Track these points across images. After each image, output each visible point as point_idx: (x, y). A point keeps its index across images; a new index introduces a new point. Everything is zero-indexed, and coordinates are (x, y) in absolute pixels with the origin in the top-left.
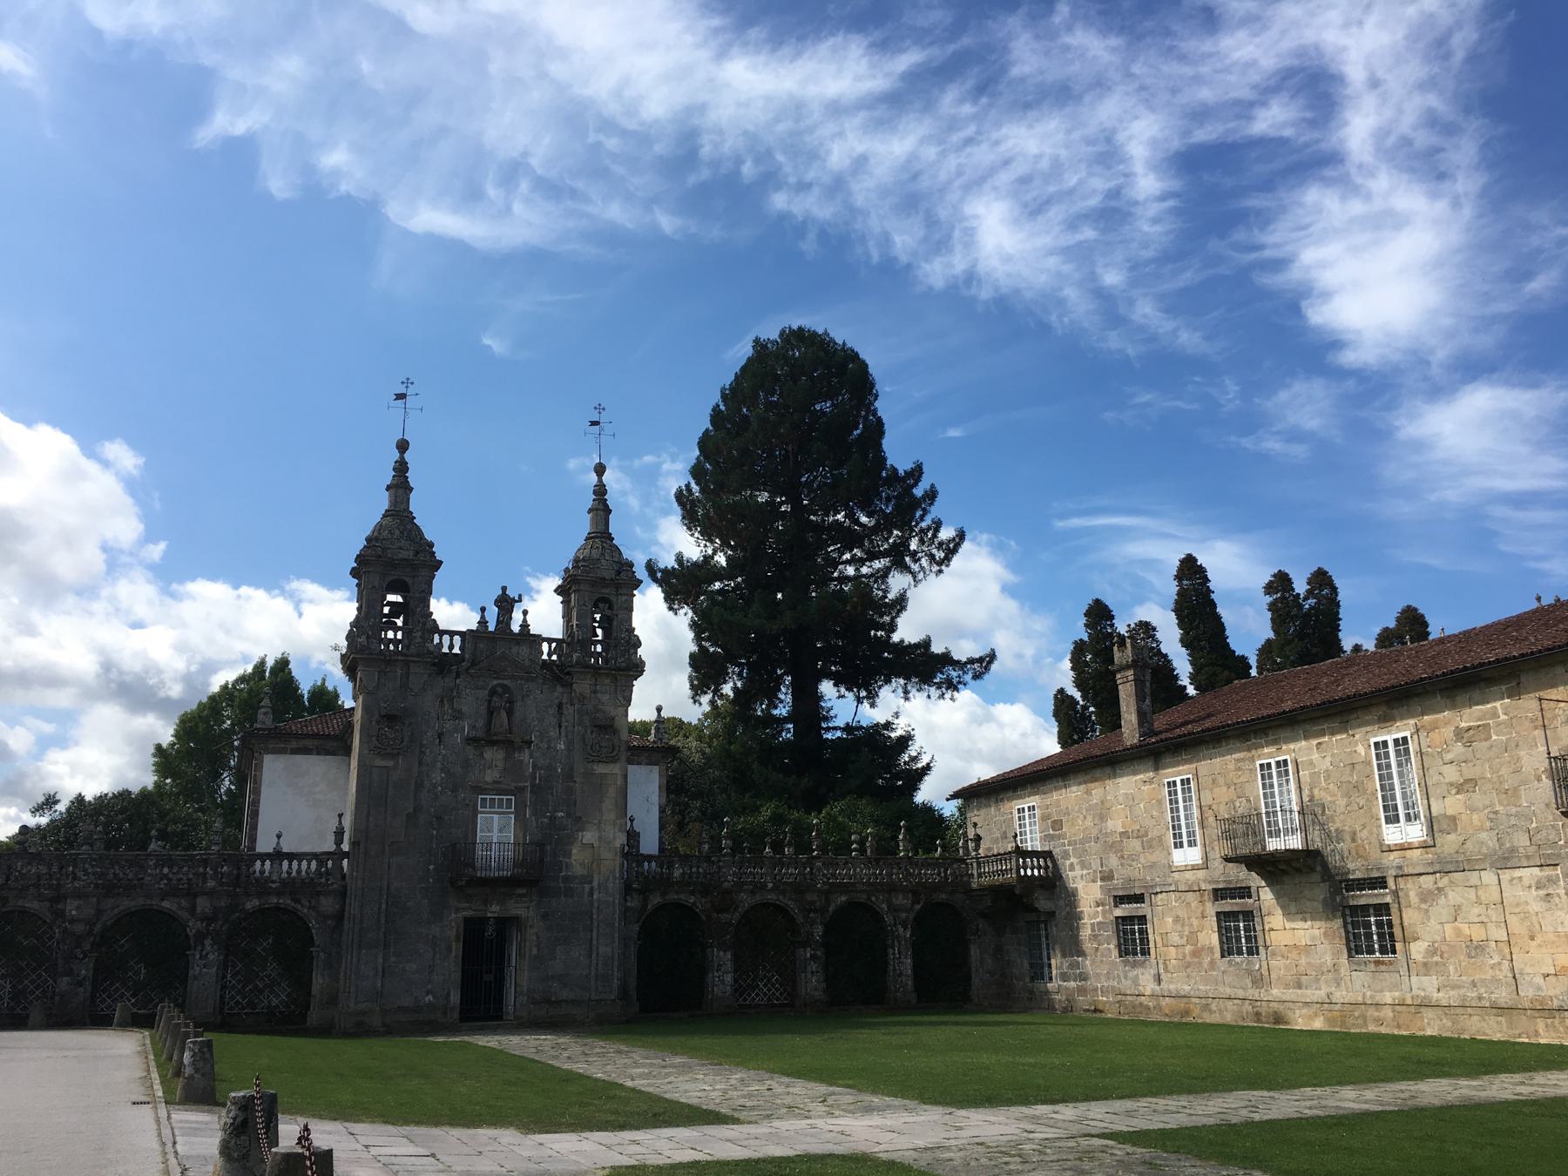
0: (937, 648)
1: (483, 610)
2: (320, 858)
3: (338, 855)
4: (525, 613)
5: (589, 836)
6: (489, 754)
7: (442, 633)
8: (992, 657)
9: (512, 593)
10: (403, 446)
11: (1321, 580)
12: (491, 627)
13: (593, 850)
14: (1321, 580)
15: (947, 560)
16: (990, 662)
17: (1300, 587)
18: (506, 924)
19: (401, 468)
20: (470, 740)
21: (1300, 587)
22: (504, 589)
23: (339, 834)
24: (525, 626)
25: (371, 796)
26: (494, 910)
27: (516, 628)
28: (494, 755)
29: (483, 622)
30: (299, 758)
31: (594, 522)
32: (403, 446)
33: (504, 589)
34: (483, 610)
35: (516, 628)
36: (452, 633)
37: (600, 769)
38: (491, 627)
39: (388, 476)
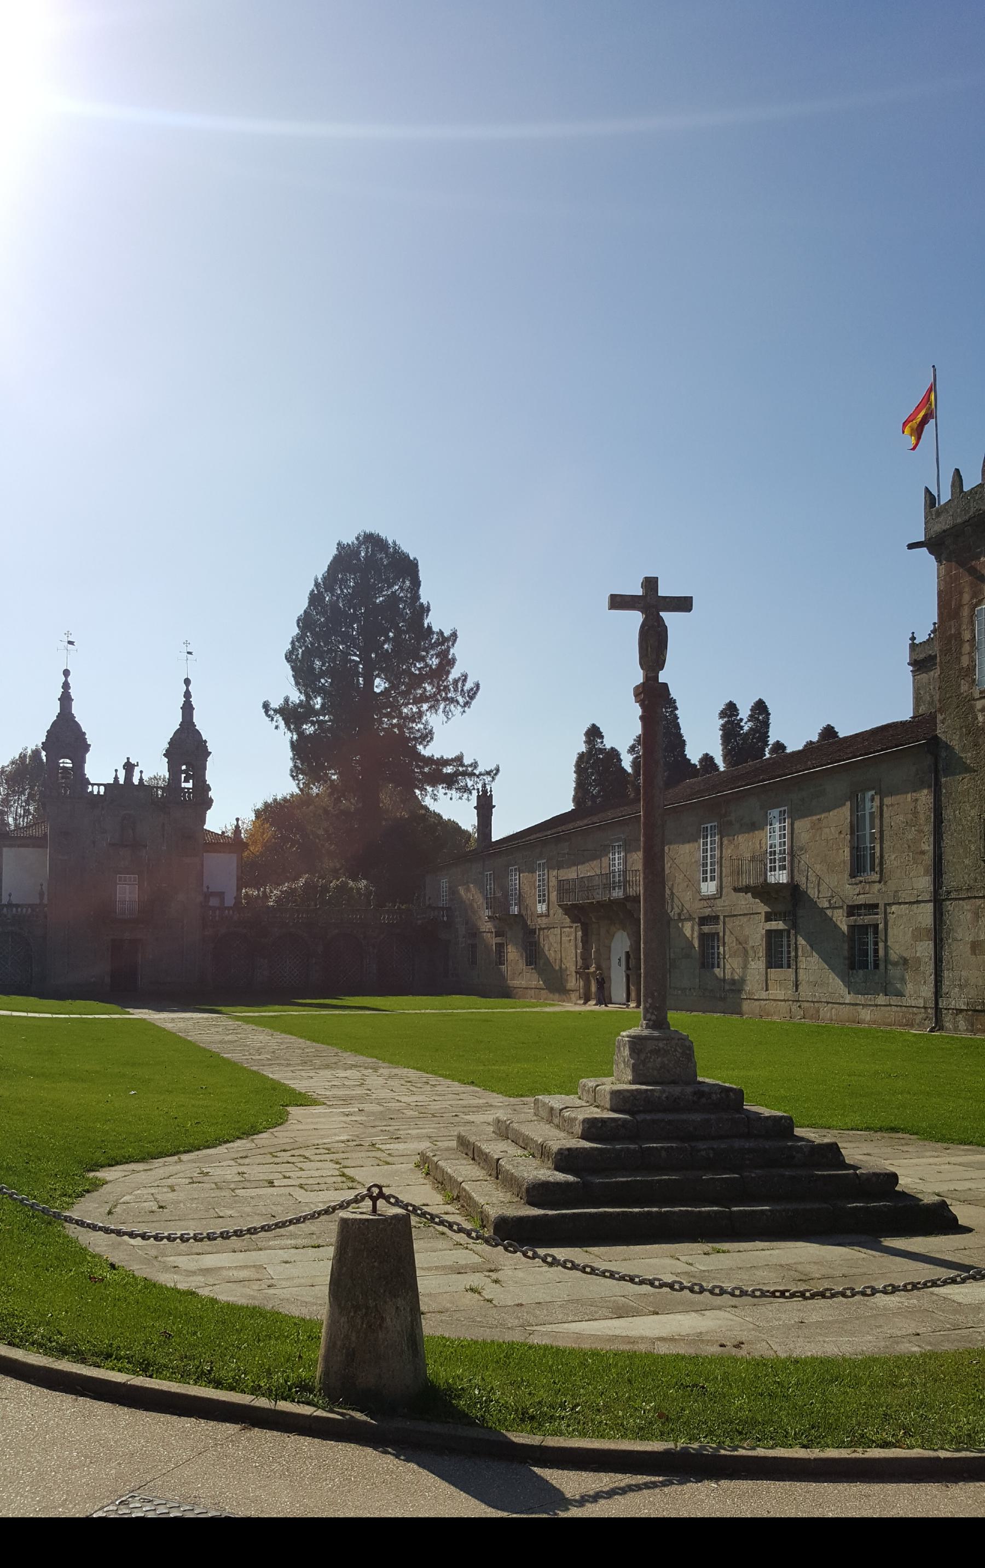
0: (467, 761)
1: (116, 771)
4: (141, 772)
7: (93, 785)
8: (498, 770)
9: (133, 761)
10: (66, 673)
11: (760, 708)
12: (122, 781)
14: (760, 708)
15: (467, 704)
16: (496, 774)
17: (744, 713)
19: (66, 686)
21: (744, 713)
22: (128, 759)
27: (136, 781)
29: (116, 778)
32: (66, 673)
33: (128, 759)
34: (116, 771)
35: (136, 781)
36: (99, 785)
38: (122, 781)
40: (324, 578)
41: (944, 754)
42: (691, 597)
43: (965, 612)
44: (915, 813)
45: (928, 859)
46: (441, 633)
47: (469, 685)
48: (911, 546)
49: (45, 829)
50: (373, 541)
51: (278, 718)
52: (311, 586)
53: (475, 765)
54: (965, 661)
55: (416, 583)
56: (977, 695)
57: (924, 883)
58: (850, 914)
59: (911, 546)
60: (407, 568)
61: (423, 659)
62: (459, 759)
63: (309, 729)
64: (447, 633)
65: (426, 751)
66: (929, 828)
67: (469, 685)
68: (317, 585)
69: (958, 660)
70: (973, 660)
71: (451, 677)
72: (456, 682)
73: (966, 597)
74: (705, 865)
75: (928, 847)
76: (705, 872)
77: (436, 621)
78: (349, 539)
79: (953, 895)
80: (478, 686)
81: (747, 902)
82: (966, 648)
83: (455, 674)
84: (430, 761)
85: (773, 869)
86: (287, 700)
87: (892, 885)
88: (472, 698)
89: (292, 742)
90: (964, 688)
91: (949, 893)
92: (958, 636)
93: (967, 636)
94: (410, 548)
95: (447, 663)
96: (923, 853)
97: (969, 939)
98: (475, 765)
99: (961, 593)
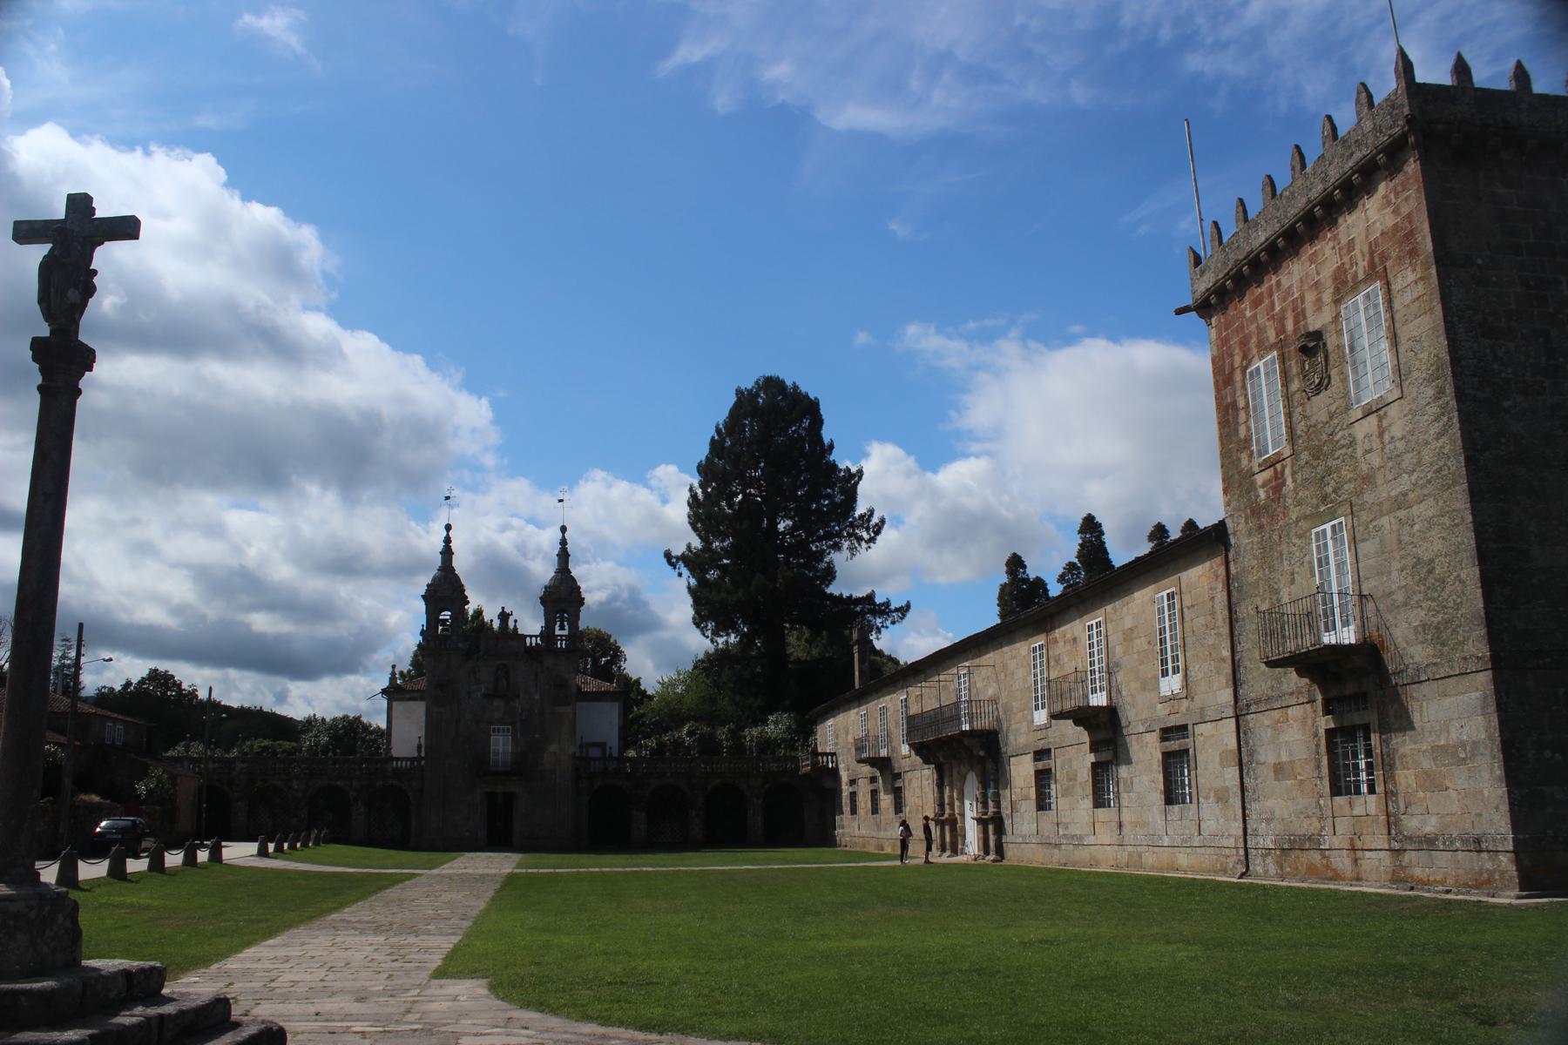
0: (879, 600)
2: (412, 760)
3: (419, 759)
5: (553, 748)
6: (496, 703)
8: (908, 606)
9: (507, 610)
13: (558, 753)
15: (872, 540)
18: (510, 798)
20: (486, 696)
23: (419, 747)
24: (516, 629)
25: (432, 726)
26: (500, 789)
28: (498, 703)
30: (411, 703)
31: (560, 563)
37: (560, 710)
39: (440, 545)
40: (726, 424)
41: (1233, 541)
42: (136, 237)
43: (1238, 376)
44: (1213, 613)
45: (1227, 668)
46: (848, 470)
47: (875, 520)
48: (1179, 312)
49: (422, 684)
50: (772, 384)
51: (681, 564)
52: (712, 432)
53: (887, 604)
54: (1242, 431)
55: (818, 422)
56: (1256, 469)
57: (1226, 695)
58: (1163, 739)
59: (1179, 312)
60: (809, 409)
61: (828, 496)
62: (870, 598)
63: (712, 575)
64: (854, 470)
65: (834, 589)
66: (1225, 630)
67: (875, 520)
68: (718, 431)
69: (1236, 431)
70: (1249, 429)
71: (857, 514)
72: (862, 517)
73: (1237, 360)
74: (1036, 690)
75: (1226, 653)
76: (1036, 699)
77: (843, 460)
78: (748, 384)
79: (1253, 709)
80: (883, 521)
81: (1069, 729)
82: (1242, 416)
83: (860, 510)
84: (839, 600)
85: (1094, 691)
86: (689, 546)
87: (1198, 703)
88: (877, 533)
89: (689, 588)
90: (1244, 462)
91: (1248, 706)
92: (1234, 404)
93: (1241, 403)
94: (809, 388)
95: (851, 497)
96: (1223, 660)
97: (1271, 760)
98: (887, 604)
99: (1232, 356)
